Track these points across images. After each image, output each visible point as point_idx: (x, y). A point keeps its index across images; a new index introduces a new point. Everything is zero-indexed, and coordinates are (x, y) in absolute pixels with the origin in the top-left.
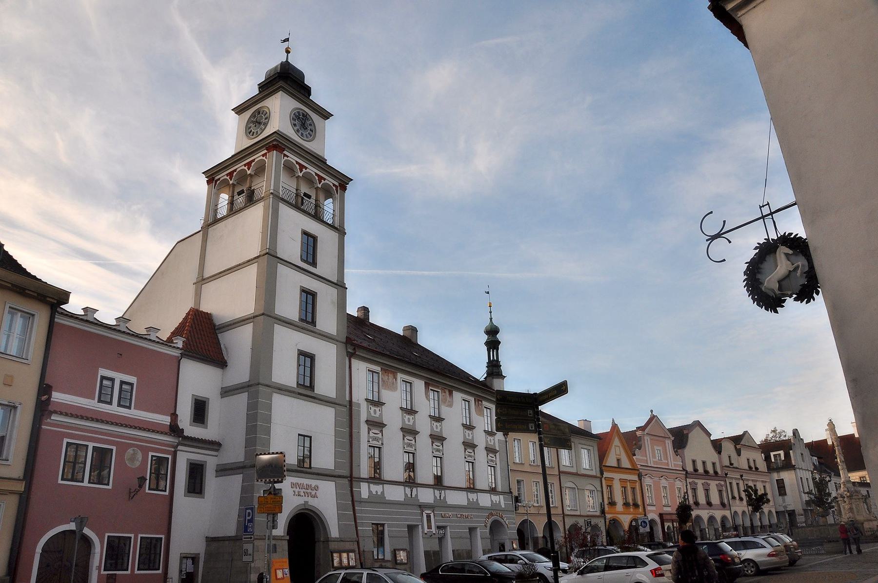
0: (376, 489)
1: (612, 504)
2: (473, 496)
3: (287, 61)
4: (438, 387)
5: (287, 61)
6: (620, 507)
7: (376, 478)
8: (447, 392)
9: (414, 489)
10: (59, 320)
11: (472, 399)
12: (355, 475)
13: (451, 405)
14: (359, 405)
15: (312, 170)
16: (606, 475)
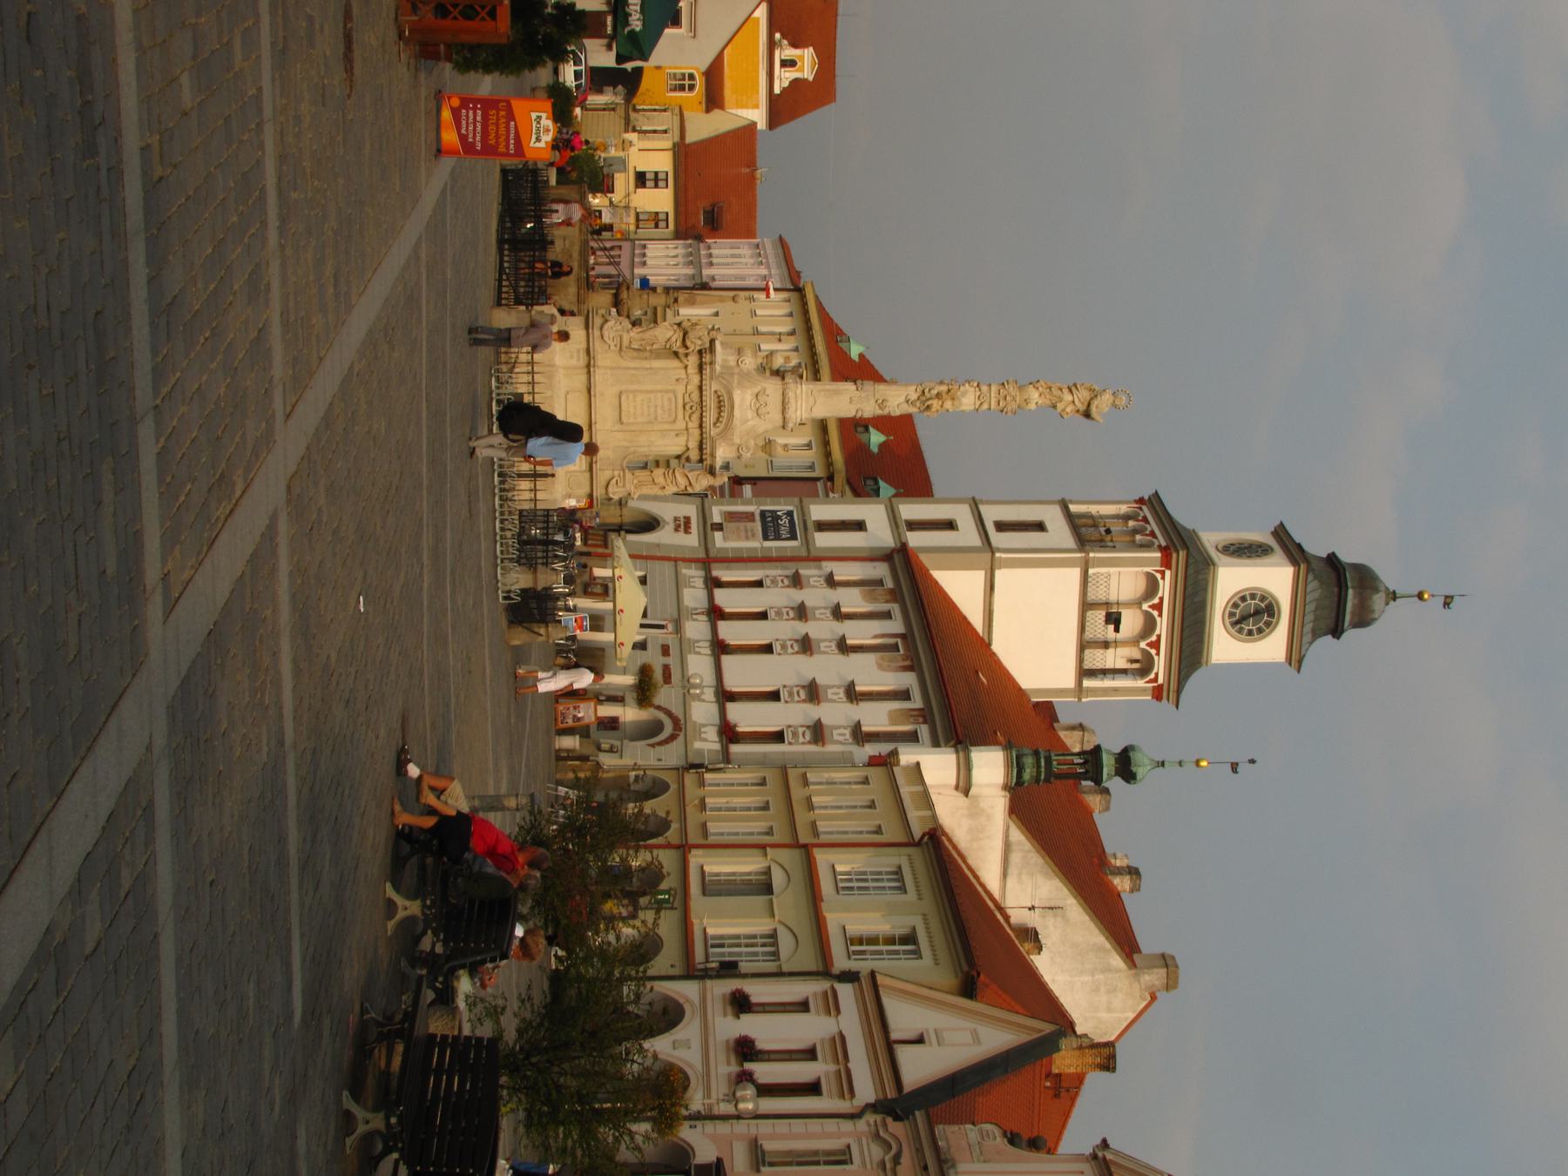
0: (700, 583)
1: (741, 1004)
2: (709, 694)
3: (1394, 596)
4: (907, 648)
5: (1394, 596)
6: (731, 1027)
7: (713, 583)
8: (908, 663)
9: (704, 618)
10: (820, 485)
11: (917, 702)
12: (713, 565)
13: (880, 667)
14: (820, 568)
15: (1154, 526)
16: (845, 991)
